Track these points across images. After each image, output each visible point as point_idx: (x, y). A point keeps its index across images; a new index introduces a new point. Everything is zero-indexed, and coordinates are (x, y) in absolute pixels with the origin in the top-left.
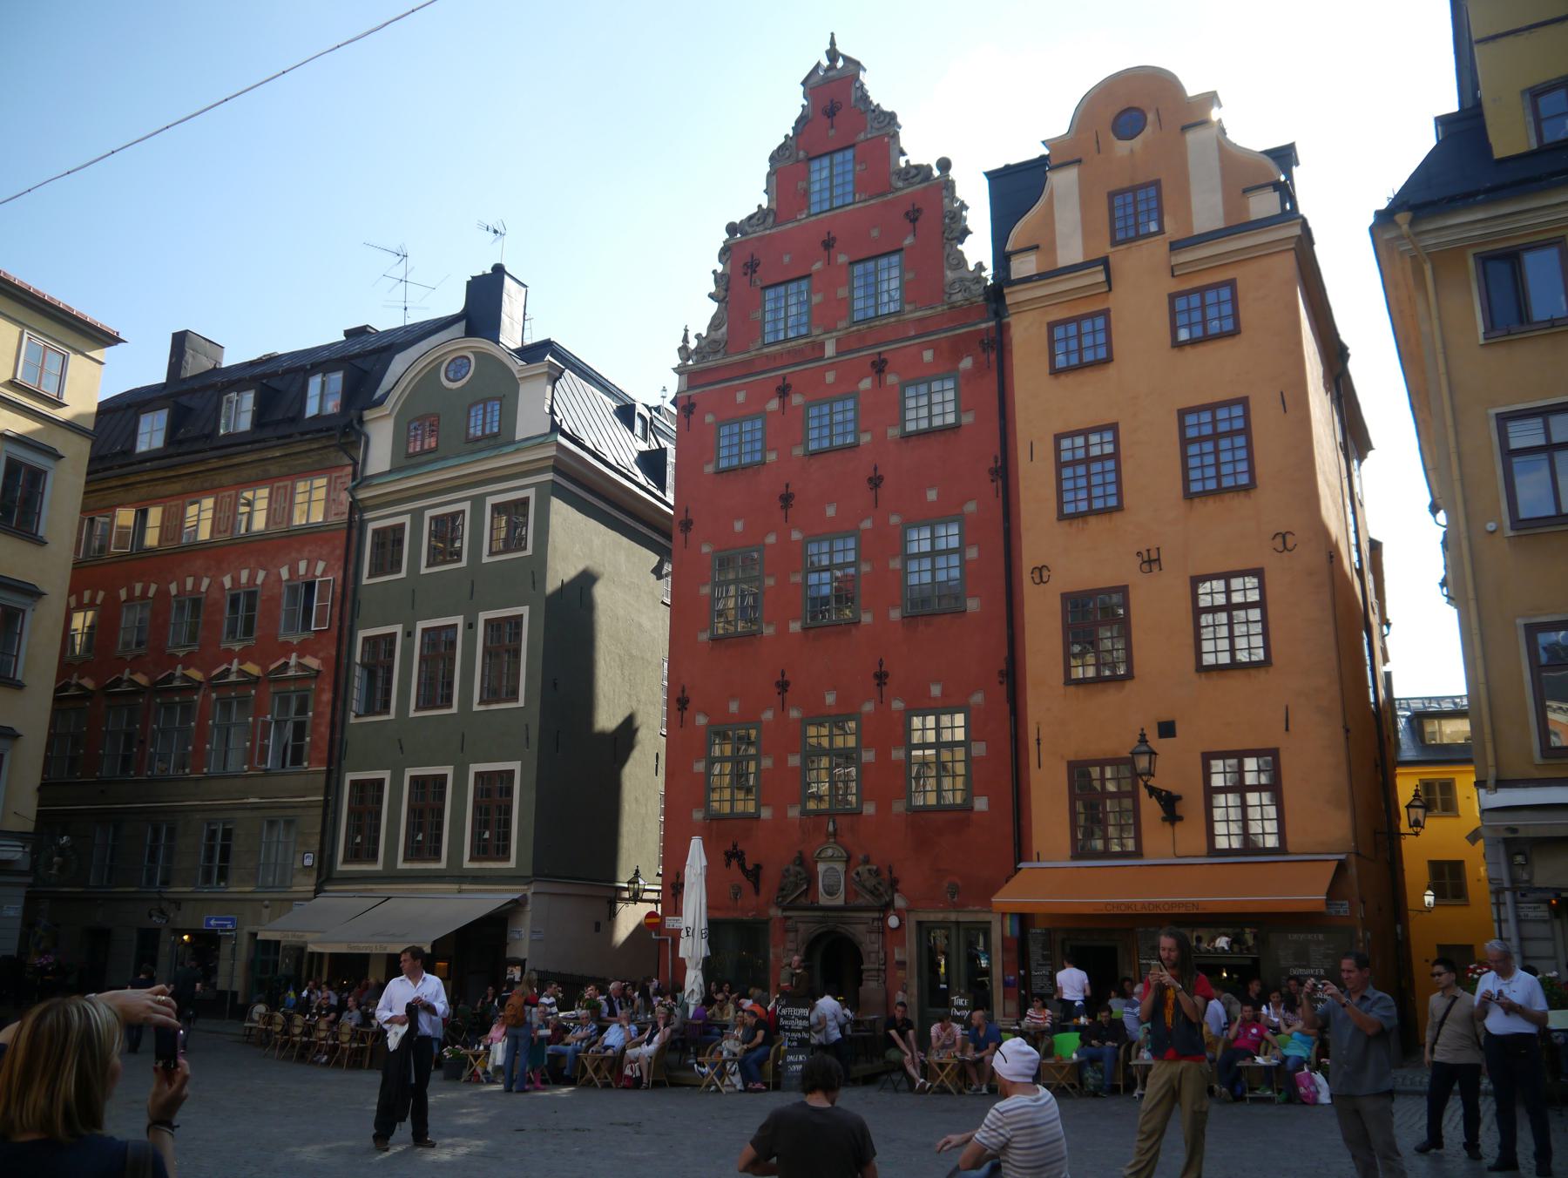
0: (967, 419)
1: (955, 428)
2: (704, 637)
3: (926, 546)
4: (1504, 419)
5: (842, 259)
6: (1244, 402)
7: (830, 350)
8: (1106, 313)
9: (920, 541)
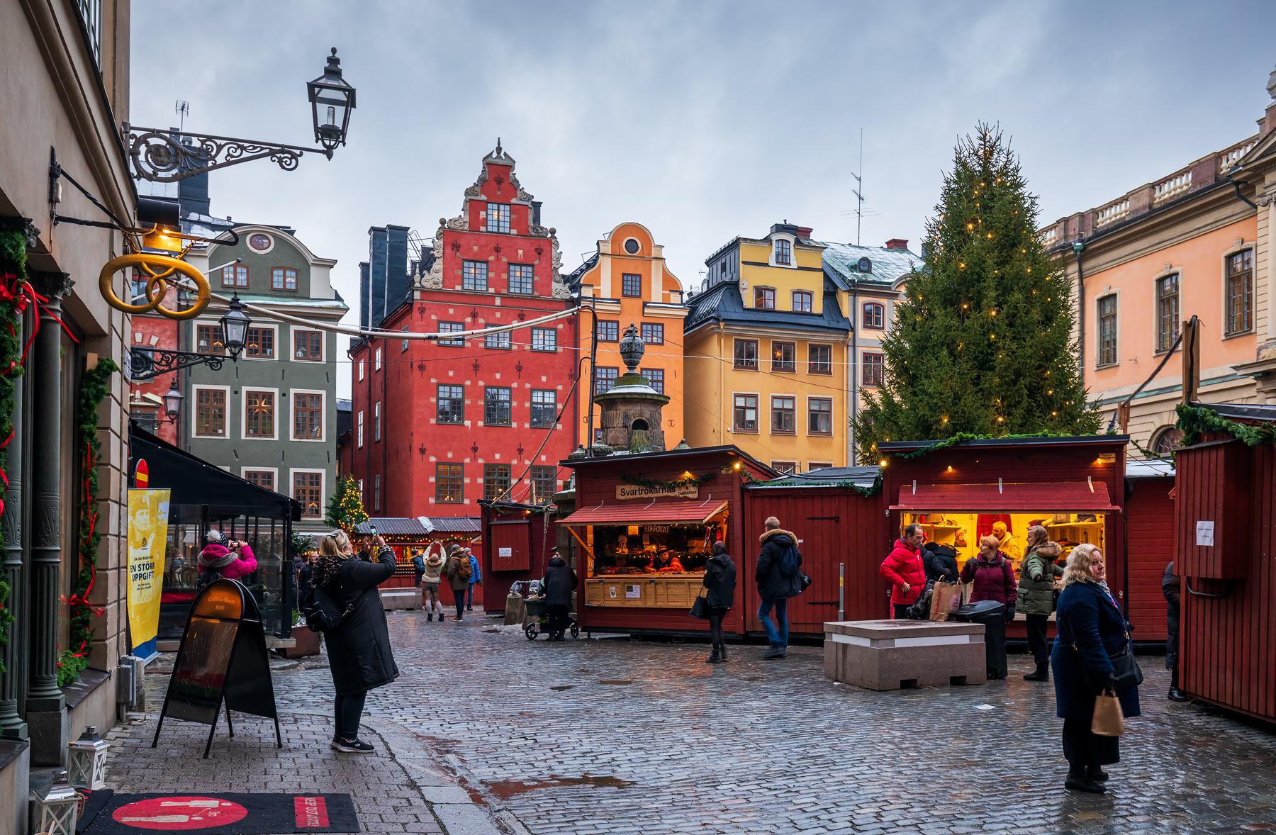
0: (560, 349)
1: (555, 352)
2: (433, 421)
3: (540, 400)
4: (736, 396)
5: (504, 260)
6: (663, 370)
7: (498, 302)
8: (617, 322)
9: (537, 397)
